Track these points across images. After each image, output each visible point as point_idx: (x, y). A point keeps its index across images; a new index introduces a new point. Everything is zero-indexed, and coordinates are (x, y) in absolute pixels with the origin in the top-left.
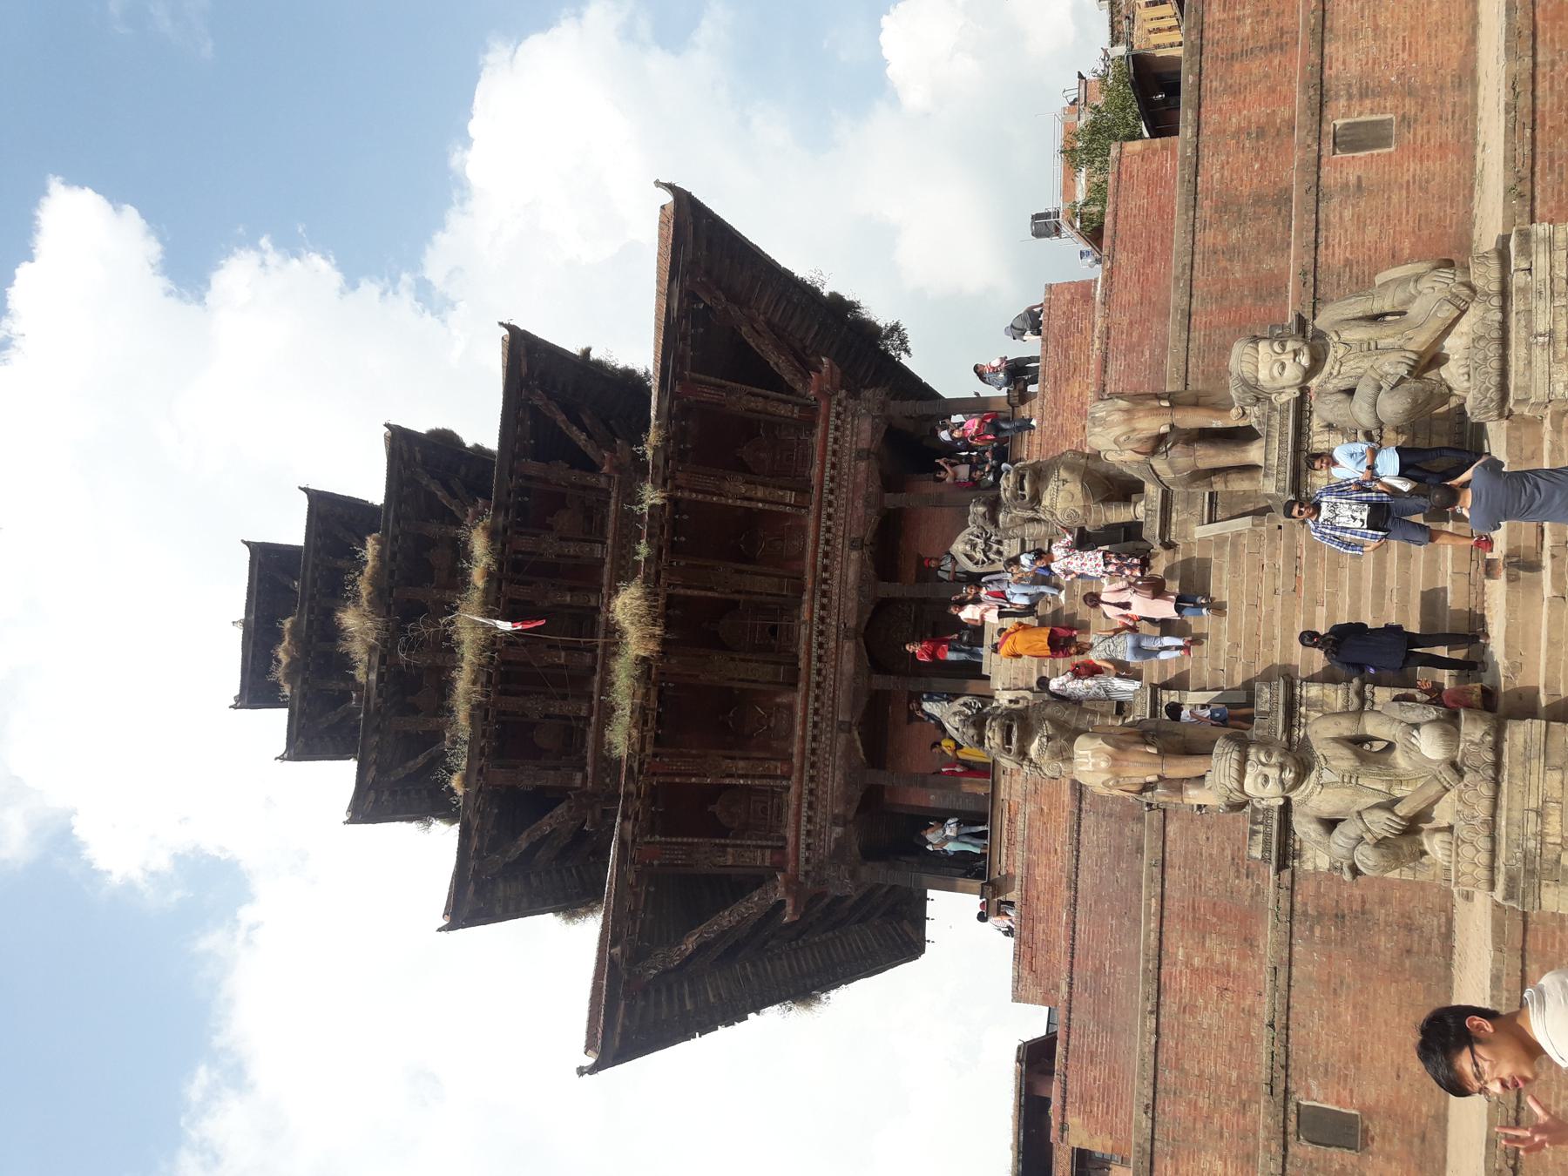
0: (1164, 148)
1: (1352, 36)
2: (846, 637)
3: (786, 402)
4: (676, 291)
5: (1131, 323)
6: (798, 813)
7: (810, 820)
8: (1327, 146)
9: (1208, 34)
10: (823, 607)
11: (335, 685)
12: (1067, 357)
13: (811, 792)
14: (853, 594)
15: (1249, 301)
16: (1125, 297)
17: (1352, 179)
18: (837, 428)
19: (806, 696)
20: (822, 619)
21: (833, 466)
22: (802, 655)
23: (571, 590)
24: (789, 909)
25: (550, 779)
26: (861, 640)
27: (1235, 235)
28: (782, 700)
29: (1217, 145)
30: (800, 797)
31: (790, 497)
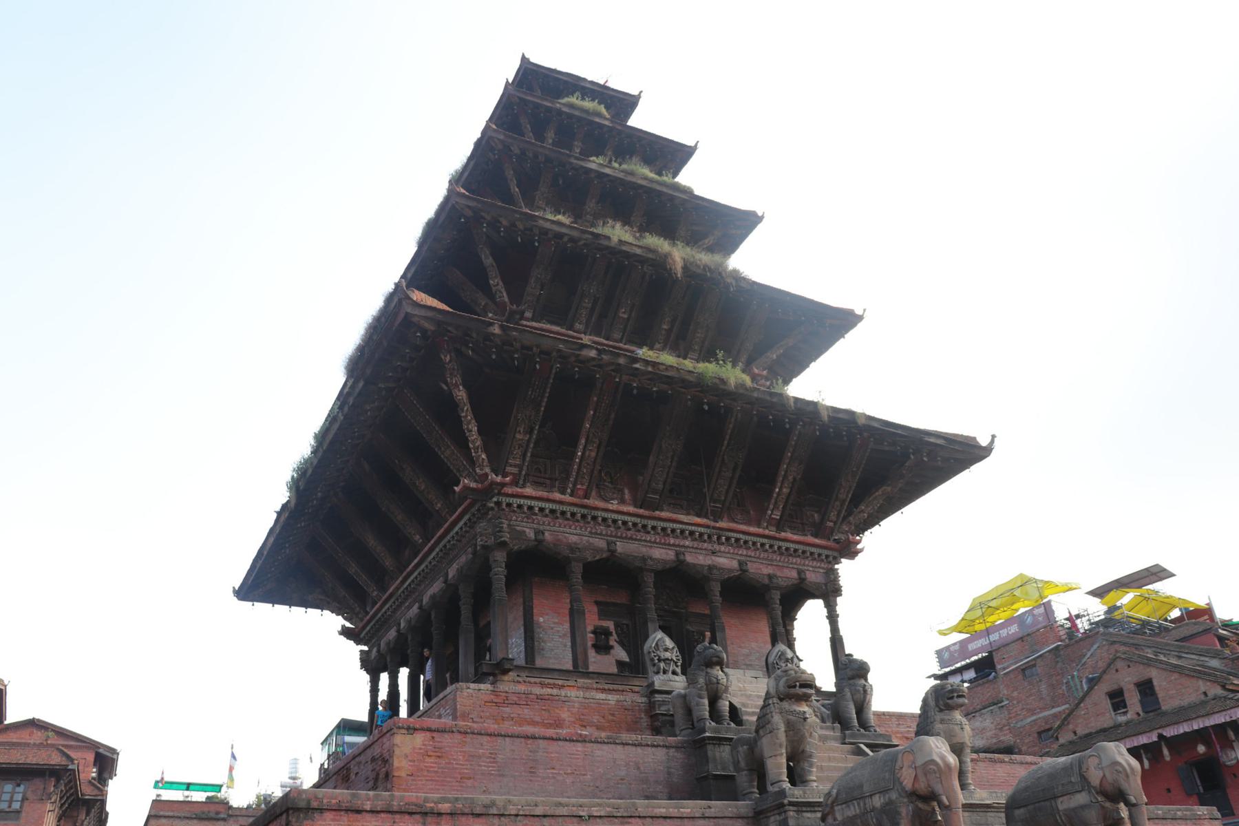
2: (677, 554)
3: (838, 515)
4: (940, 442)
6: (548, 500)
7: (541, 510)
10: (701, 535)
11: (550, 136)
13: (563, 513)
18: (820, 555)
20: (692, 533)
21: (796, 551)
22: (664, 514)
23: (669, 331)
24: (473, 485)
28: (627, 496)
30: (561, 502)
31: (777, 515)
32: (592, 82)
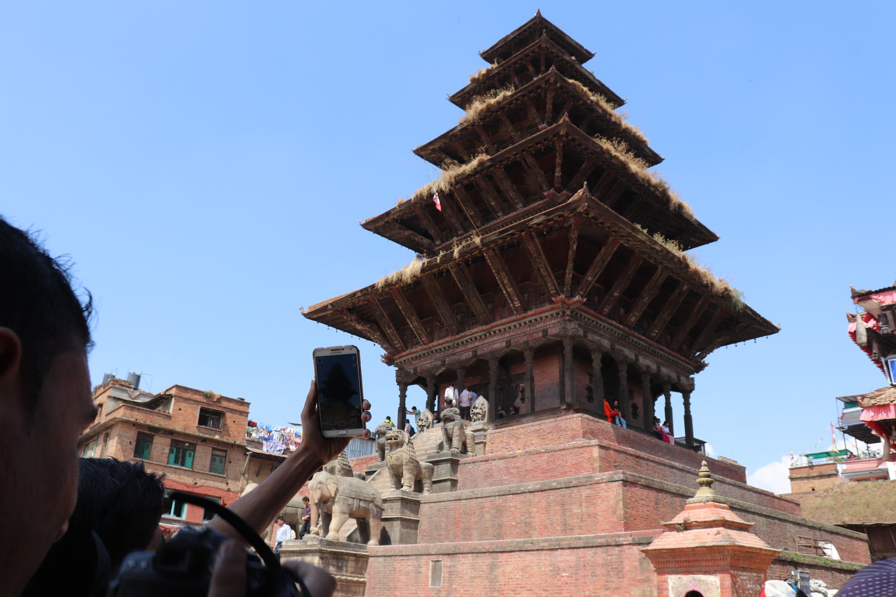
0: (594, 469)
1: (473, 567)
3: (554, 285)
5: (518, 467)
8: (435, 558)
9: (575, 490)
10: (481, 337)
12: (549, 433)
14: (489, 349)
15: (462, 526)
16: (528, 462)
17: (422, 570)
18: (552, 315)
19: (447, 342)
20: (476, 338)
21: (536, 320)
25: (432, 232)
26: (474, 360)
27: (488, 516)
29: (524, 502)
31: (517, 304)
32: (513, 33)
